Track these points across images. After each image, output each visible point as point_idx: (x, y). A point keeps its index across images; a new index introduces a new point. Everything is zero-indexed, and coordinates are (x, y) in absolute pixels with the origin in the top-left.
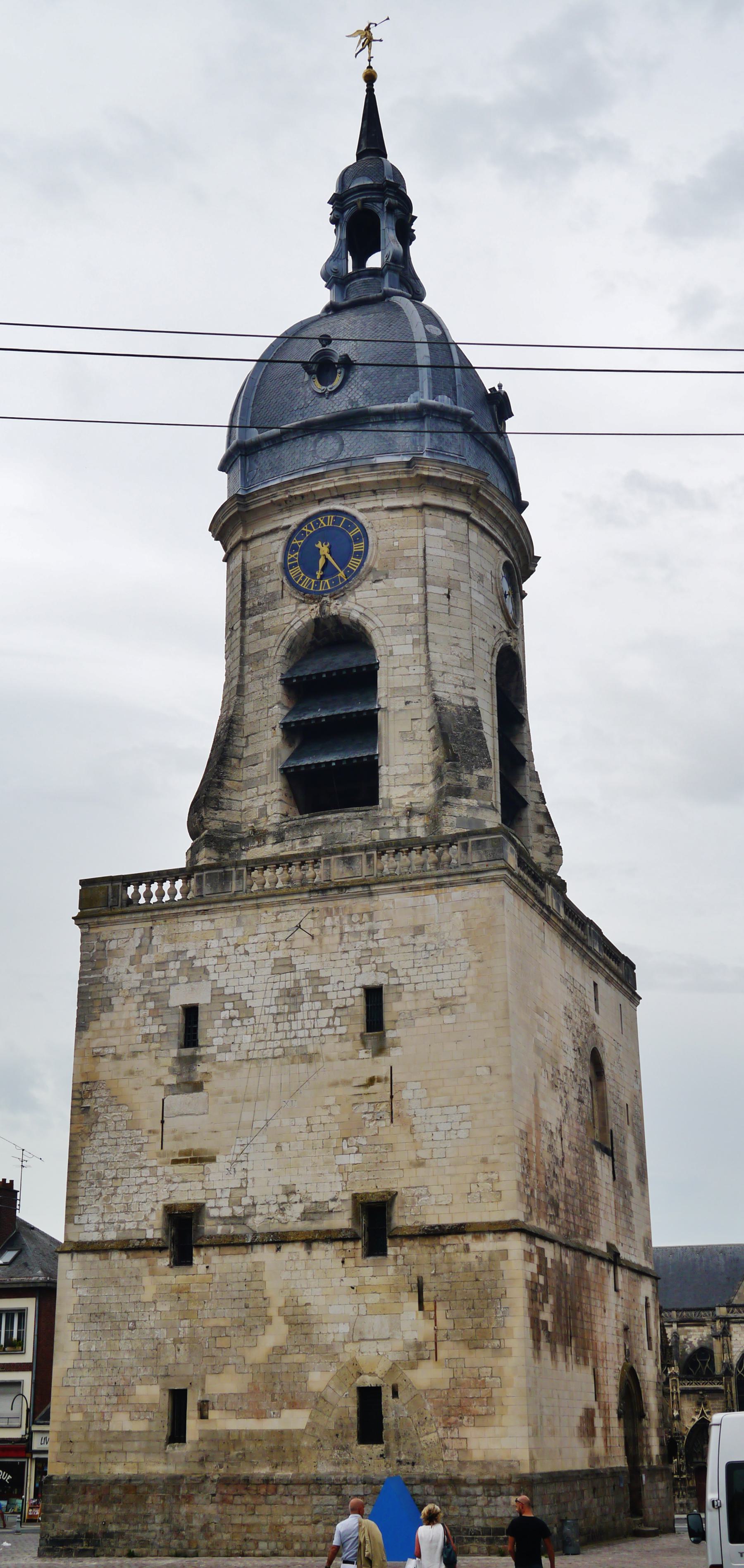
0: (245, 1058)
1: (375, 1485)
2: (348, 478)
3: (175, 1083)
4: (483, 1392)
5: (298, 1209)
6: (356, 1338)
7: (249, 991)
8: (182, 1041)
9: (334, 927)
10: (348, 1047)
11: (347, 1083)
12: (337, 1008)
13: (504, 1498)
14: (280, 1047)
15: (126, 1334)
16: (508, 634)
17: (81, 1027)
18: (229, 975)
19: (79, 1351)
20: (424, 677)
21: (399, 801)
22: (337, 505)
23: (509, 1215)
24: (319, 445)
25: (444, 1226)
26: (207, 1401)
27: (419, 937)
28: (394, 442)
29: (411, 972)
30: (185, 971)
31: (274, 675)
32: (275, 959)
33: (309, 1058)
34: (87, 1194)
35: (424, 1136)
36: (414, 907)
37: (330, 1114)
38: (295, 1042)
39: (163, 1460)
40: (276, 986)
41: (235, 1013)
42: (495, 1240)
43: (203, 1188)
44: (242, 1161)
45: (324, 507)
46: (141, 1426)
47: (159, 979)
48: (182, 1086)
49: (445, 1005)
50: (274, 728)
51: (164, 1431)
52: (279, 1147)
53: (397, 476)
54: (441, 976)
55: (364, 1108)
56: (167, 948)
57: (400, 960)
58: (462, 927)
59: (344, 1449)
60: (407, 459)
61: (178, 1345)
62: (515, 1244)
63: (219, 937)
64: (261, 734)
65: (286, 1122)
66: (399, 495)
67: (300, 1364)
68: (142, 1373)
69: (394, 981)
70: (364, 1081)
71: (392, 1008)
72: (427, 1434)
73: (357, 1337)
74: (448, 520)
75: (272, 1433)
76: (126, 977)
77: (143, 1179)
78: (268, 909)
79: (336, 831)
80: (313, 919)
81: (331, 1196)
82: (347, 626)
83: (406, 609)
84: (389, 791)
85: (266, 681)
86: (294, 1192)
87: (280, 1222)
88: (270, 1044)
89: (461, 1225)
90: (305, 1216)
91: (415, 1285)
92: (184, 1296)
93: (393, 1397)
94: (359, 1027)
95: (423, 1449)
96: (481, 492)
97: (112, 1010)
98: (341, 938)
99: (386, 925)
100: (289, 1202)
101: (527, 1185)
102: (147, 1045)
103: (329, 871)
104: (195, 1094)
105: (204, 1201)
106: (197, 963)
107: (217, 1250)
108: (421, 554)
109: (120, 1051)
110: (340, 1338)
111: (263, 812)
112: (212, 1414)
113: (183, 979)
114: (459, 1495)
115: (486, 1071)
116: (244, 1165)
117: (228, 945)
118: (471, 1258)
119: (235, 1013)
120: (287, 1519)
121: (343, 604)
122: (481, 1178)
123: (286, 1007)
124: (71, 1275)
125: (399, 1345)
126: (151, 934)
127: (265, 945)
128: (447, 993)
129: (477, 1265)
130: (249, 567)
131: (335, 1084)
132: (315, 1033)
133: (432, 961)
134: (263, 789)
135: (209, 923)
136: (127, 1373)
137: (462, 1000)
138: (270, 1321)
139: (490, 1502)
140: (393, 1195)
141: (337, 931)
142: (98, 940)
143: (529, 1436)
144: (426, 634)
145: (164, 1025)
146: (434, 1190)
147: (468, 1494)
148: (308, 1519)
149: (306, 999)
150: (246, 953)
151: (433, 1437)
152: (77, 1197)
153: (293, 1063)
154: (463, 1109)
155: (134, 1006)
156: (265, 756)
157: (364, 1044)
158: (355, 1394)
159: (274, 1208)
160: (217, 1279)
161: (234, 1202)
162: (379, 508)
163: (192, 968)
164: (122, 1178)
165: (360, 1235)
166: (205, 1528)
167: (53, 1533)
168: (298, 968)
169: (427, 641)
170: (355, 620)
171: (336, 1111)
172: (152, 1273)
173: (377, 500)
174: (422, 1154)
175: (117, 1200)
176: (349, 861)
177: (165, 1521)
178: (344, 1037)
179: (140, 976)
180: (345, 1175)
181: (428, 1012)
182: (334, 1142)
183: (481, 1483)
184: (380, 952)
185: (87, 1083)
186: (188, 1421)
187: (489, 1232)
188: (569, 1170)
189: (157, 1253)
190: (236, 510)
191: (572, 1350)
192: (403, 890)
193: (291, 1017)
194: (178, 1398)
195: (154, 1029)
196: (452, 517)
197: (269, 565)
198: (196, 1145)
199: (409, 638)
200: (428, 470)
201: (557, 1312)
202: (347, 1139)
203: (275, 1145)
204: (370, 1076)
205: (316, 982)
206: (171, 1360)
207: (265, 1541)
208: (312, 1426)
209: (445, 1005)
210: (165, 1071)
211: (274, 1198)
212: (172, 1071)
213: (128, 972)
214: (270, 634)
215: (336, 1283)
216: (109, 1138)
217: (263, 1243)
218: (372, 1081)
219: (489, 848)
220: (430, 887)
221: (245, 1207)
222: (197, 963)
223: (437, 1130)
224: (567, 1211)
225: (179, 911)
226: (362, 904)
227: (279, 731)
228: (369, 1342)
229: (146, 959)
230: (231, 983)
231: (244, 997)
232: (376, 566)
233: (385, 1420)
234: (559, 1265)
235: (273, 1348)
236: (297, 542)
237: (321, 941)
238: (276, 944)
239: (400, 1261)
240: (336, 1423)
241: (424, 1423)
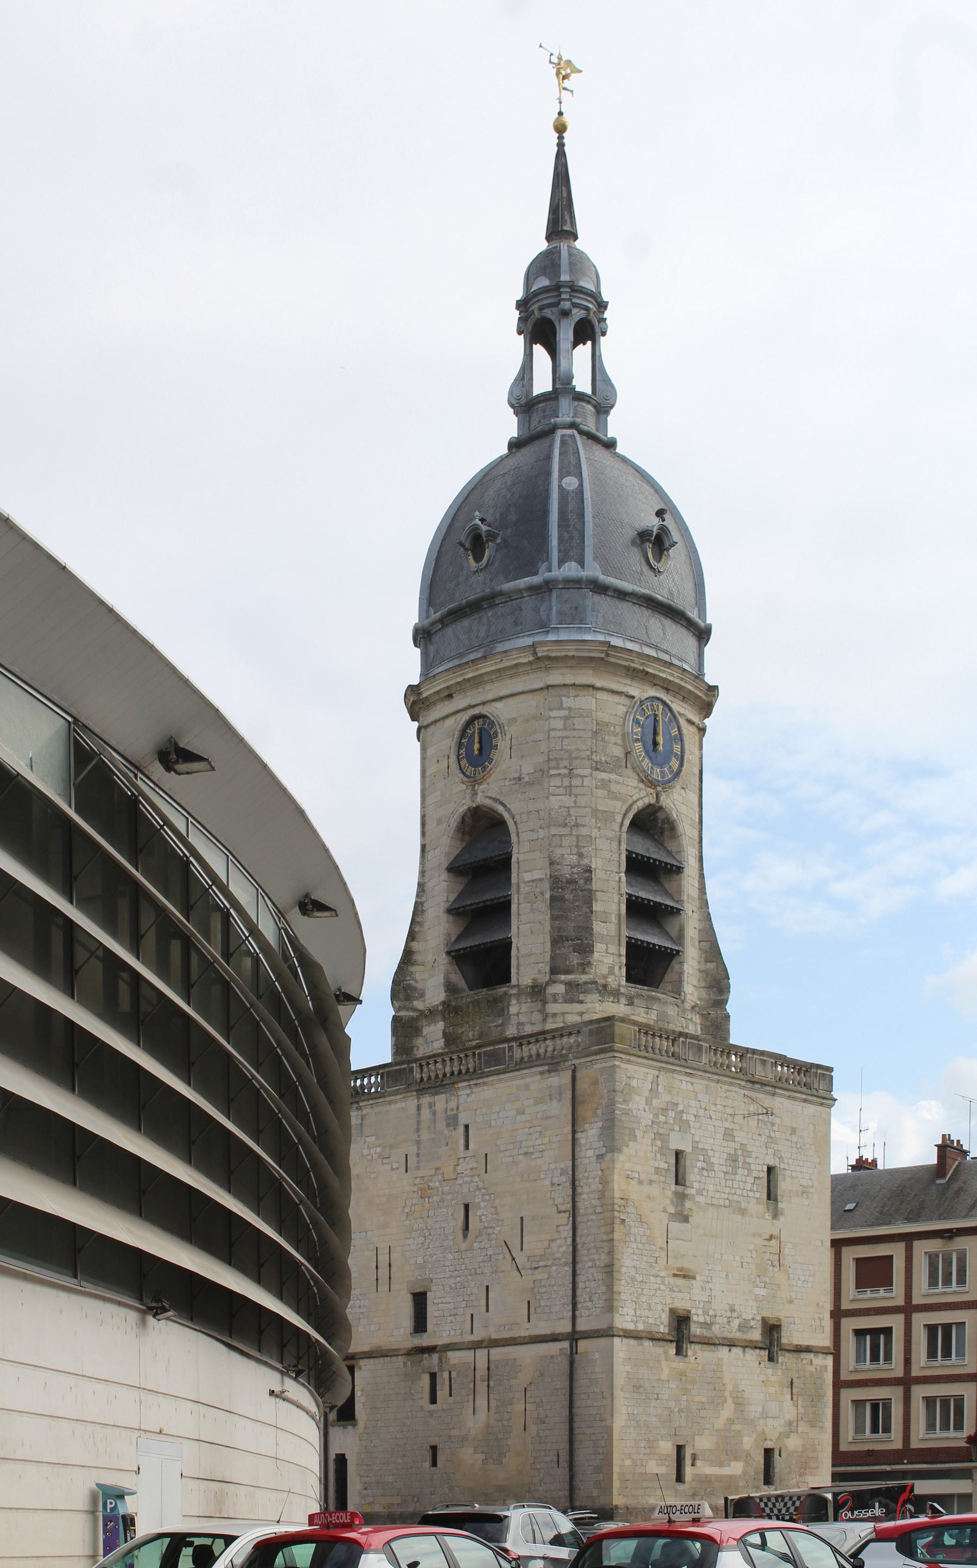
0: (710, 1202)
3: (674, 1212)
4: (815, 1455)
5: (736, 1323)
6: (764, 1417)
7: (712, 1150)
11: (760, 1235)
12: (755, 1178)
15: (653, 1402)
27: (793, 1136)
29: (791, 1162)
32: (726, 1128)
33: (742, 1212)
36: (792, 1112)
38: (735, 1197)
39: (674, 1494)
52: (727, 1275)
56: (667, 1098)
63: (696, 1099)
64: (610, 895)
67: (739, 1431)
68: (663, 1432)
70: (768, 1237)
71: (784, 1186)
72: (792, 1479)
73: (765, 1415)
75: (725, 1476)
76: (644, 1114)
77: (657, 1286)
78: (722, 1085)
86: (734, 1310)
89: (808, 1346)
90: (741, 1328)
97: (636, 1140)
98: (758, 1123)
104: (685, 1224)
107: (700, 1346)
109: (642, 1177)
110: (757, 1415)
112: (698, 1463)
113: (677, 1128)
117: (701, 1108)
118: (812, 1368)
119: (704, 1165)
125: (782, 1422)
131: (754, 1235)
135: (689, 1084)
137: (812, 1190)
138: (725, 1401)
145: (667, 1163)
146: (797, 1321)
149: (740, 1166)
150: (711, 1118)
152: (620, 1293)
154: (811, 1268)
155: (649, 1141)
157: (768, 1208)
158: (763, 1453)
159: (725, 1320)
161: (706, 1313)
164: (646, 1282)
168: (737, 1139)
172: (667, 1359)
174: (793, 1295)
175: (644, 1299)
176: (764, 1063)
178: (758, 1200)
185: (622, 1199)
189: (669, 1343)
193: (733, 1177)
194: (680, 1449)
202: (759, 1276)
204: (770, 1233)
206: (677, 1424)
208: (744, 1472)
210: (668, 1202)
213: (645, 1111)
216: (638, 1248)
217: (723, 1345)
221: (711, 1316)
225: (678, 1068)
229: (655, 1102)
231: (710, 1153)
239: (784, 1367)
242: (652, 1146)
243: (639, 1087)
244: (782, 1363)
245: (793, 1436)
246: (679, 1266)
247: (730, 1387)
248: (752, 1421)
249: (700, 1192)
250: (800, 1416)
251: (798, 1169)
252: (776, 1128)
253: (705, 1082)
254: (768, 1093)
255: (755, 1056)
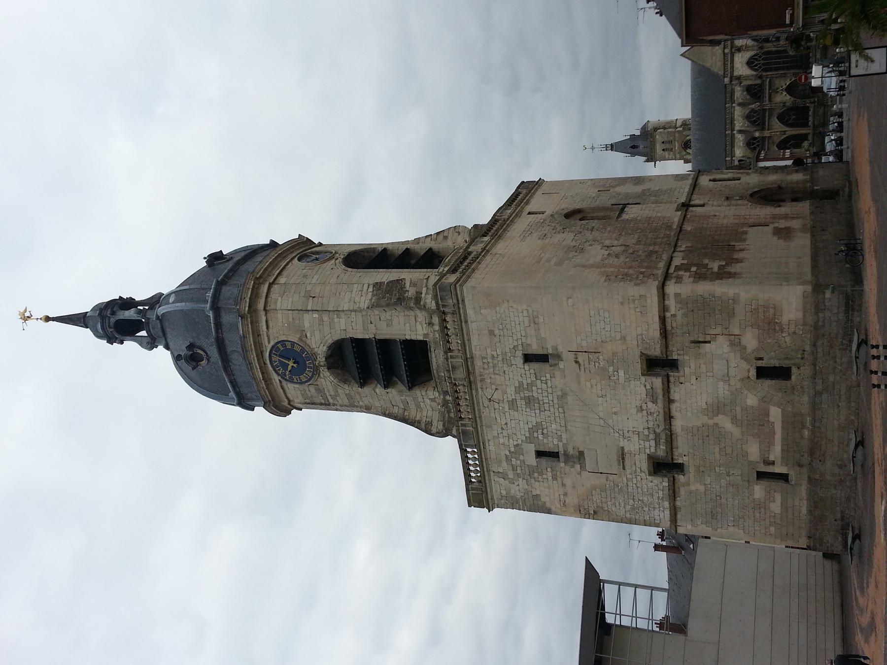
0: (565, 428)
1: (816, 373)
2: (252, 350)
4: (761, 310)
5: (650, 405)
7: (527, 424)
8: (556, 459)
9: (491, 378)
10: (557, 373)
13: (826, 301)
14: (558, 409)
15: (723, 501)
16: (336, 259)
17: (549, 511)
18: (518, 433)
19: (734, 526)
20: (357, 313)
21: (424, 329)
22: (267, 355)
23: (654, 291)
24: (235, 363)
25: (660, 327)
26: (764, 461)
27: (495, 333)
28: (232, 324)
29: (515, 338)
30: (517, 456)
31: (359, 391)
32: (509, 409)
33: (564, 395)
34: (643, 515)
35: (608, 335)
36: (479, 335)
37: (596, 385)
38: (556, 401)
40: (524, 409)
41: (540, 431)
42: (669, 300)
43: (639, 454)
44: (623, 433)
45: (268, 362)
46: (778, 497)
47: (522, 470)
48: (581, 461)
49: (534, 320)
50: (387, 393)
51: (781, 484)
52: (615, 413)
53: (249, 324)
54: (517, 322)
55: (592, 366)
56: (504, 464)
57: (509, 343)
58: (489, 310)
59: (794, 389)
60: (240, 318)
61: (730, 474)
62: (672, 288)
64: (391, 398)
65: (601, 408)
66: (260, 322)
69: (520, 348)
70: (577, 366)
71: (535, 349)
72: (786, 342)
73: (726, 378)
74: (273, 296)
75: (783, 428)
76: (521, 486)
79: (442, 364)
80: (486, 389)
81: (642, 386)
82: (331, 352)
83: (321, 320)
84: (419, 335)
85: (362, 395)
86: (641, 406)
87: (658, 415)
88: (557, 414)
90: (654, 401)
91: (695, 344)
92: (702, 469)
93: (763, 360)
94: (546, 367)
95: (795, 345)
96: (258, 276)
98: (497, 374)
99: (489, 350)
100: (646, 410)
101: (637, 278)
102: (558, 478)
103: (460, 378)
105: (646, 454)
106: (512, 449)
107: (674, 450)
108: (291, 312)
110: (727, 387)
111: (433, 400)
112: (772, 458)
113: (521, 457)
114: (824, 326)
115: (570, 301)
116: (625, 432)
118: (680, 314)
119: (540, 431)
120: (836, 422)
121: (319, 354)
122: (632, 306)
123: (536, 405)
124: (689, 527)
125: (732, 355)
126: (496, 472)
127: (501, 414)
128: (526, 319)
129: (683, 311)
130: (303, 401)
131: (579, 382)
132: (550, 390)
133: (508, 326)
134: (420, 399)
135: (490, 442)
136: (746, 501)
137: (530, 311)
139: (828, 309)
140: (642, 354)
141: (493, 376)
142: (501, 499)
143: (788, 285)
144: (334, 311)
146: (639, 331)
147: (824, 321)
148: (836, 410)
150: (506, 424)
151: (788, 339)
153: (567, 403)
154: (592, 313)
155: (536, 483)
156: (402, 398)
157: (555, 365)
158: (760, 381)
159: (650, 418)
160: (691, 451)
162: (267, 333)
163: (515, 453)
164: (634, 496)
165: (666, 373)
166: (840, 467)
167: (840, 547)
168: (514, 397)
169: (339, 311)
170: (327, 348)
171: (594, 382)
172: (689, 485)
173: (263, 334)
174: (618, 337)
175: (645, 499)
176: (454, 368)
177: (835, 488)
179: (521, 480)
180: (630, 379)
181: (537, 330)
182: (612, 384)
183: (816, 313)
184: (504, 354)
185: (580, 511)
186: (776, 472)
187: (664, 303)
188: (631, 241)
189: (676, 481)
190: (273, 407)
191: (738, 245)
192: (469, 340)
194: (761, 475)
195: (550, 474)
196: (272, 293)
197: (301, 391)
198: (614, 457)
199: (336, 320)
200: (245, 307)
201: (714, 257)
202: (610, 377)
203: (613, 415)
205: (521, 388)
206: (739, 478)
207: (849, 435)
208: (779, 405)
209: (534, 320)
210: (572, 470)
211: (644, 417)
212: (573, 466)
213: (518, 485)
214: (338, 392)
215: (694, 387)
217: (671, 425)
218: (577, 362)
219: (444, 294)
220: (467, 326)
222: (512, 449)
223: (604, 328)
224: (655, 244)
226: (478, 363)
227: (389, 390)
228: (730, 372)
229: (511, 475)
230: (523, 433)
232: (298, 336)
233: (777, 365)
234: (688, 252)
235: (733, 423)
236: (287, 376)
237: (498, 385)
238: (501, 408)
239: (681, 352)
240: (778, 392)
241: (779, 344)
242: (539, 481)
243: (505, 489)
244: (678, 355)
245: (743, 342)
246: (616, 463)
247: (705, 419)
248: (732, 393)
249: (560, 438)
250: (725, 332)
251: (518, 330)
252: (494, 353)
253: (484, 427)
254: (473, 362)
255: (452, 376)
